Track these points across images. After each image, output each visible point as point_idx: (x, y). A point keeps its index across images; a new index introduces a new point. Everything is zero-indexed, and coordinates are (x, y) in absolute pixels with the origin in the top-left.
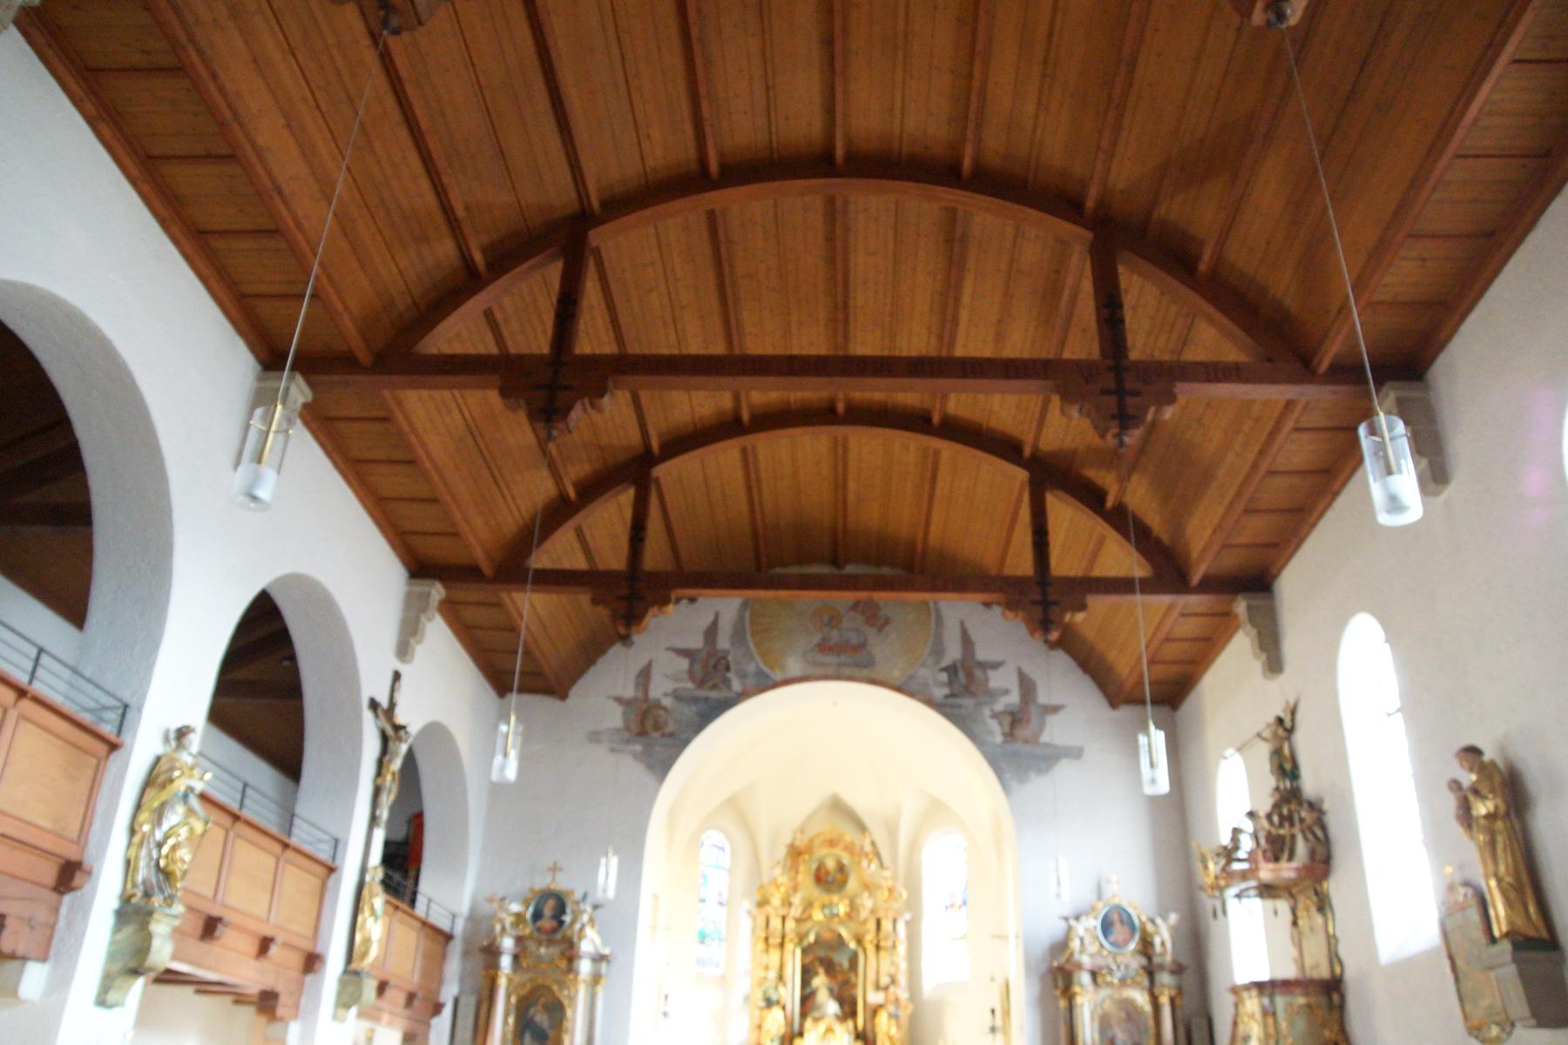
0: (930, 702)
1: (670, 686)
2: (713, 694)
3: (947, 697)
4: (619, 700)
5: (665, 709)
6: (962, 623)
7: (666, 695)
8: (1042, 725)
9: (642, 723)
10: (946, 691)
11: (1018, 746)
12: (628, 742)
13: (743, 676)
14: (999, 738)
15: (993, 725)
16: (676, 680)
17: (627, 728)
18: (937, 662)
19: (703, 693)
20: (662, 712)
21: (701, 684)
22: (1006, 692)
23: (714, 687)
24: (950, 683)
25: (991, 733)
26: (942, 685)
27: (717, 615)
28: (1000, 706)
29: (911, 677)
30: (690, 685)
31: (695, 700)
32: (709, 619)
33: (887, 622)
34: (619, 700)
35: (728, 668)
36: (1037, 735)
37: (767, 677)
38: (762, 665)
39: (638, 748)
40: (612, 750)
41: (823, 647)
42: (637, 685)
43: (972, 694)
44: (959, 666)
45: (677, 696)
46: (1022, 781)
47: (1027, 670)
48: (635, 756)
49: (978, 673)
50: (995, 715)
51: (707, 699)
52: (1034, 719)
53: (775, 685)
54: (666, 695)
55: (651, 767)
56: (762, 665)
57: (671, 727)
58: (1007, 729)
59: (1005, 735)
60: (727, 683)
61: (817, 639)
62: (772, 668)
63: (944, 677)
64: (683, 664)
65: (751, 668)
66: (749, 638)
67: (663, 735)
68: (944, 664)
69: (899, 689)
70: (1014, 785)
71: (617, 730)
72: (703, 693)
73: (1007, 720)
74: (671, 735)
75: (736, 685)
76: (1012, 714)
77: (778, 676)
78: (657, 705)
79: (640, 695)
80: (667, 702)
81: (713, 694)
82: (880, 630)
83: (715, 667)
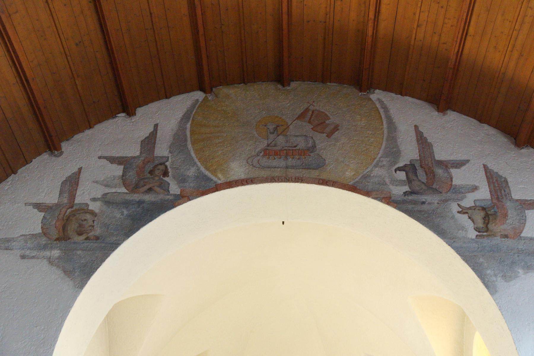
0: (389, 200)
1: (99, 191)
2: (148, 198)
3: (405, 194)
4: (38, 206)
5: (92, 213)
6: (416, 127)
7: (94, 200)
8: (523, 221)
9: (64, 228)
10: (406, 188)
11: (497, 240)
12: (45, 247)
13: (182, 180)
14: (472, 234)
15: (464, 219)
16: (107, 186)
17: (45, 233)
18: (395, 163)
19: (136, 197)
20: (88, 216)
21: (135, 188)
22: (475, 188)
23: (150, 190)
24: (409, 181)
25: (463, 228)
26: (401, 183)
27: (156, 126)
28: (468, 201)
29: (366, 177)
30: (124, 190)
31: (126, 204)
32: (145, 131)
33: (336, 128)
34: (38, 206)
35: (166, 173)
36: (517, 234)
37: (209, 179)
38: (203, 169)
39: (56, 253)
40: (23, 257)
41: (267, 152)
42: (61, 193)
43: (437, 191)
44: (417, 165)
45: (107, 200)
46: (507, 278)
47: (494, 166)
48: (50, 261)
49: (439, 171)
50: (463, 211)
51: (140, 203)
52: (512, 214)
53: (217, 188)
54: (94, 200)
55: (68, 273)
56: (203, 169)
57: (98, 231)
58: (481, 224)
59: (477, 229)
60: (165, 187)
61: (263, 145)
62: (214, 172)
63: (402, 175)
64: (118, 170)
65: (191, 172)
66: (190, 146)
67: (87, 239)
68: (401, 164)
69: (353, 189)
70: (500, 283)
71: (34, 236)
72: (136, 197)
73: (479, 216)
74: (97, 238)
75: (174, 189)
76: (484, 209)
77: (221, 179)
78: (84, 209)
79: (65, 201)
80: (95, 207)
81: (148, 198)
82: (329, 136)
83: (151, 172)
